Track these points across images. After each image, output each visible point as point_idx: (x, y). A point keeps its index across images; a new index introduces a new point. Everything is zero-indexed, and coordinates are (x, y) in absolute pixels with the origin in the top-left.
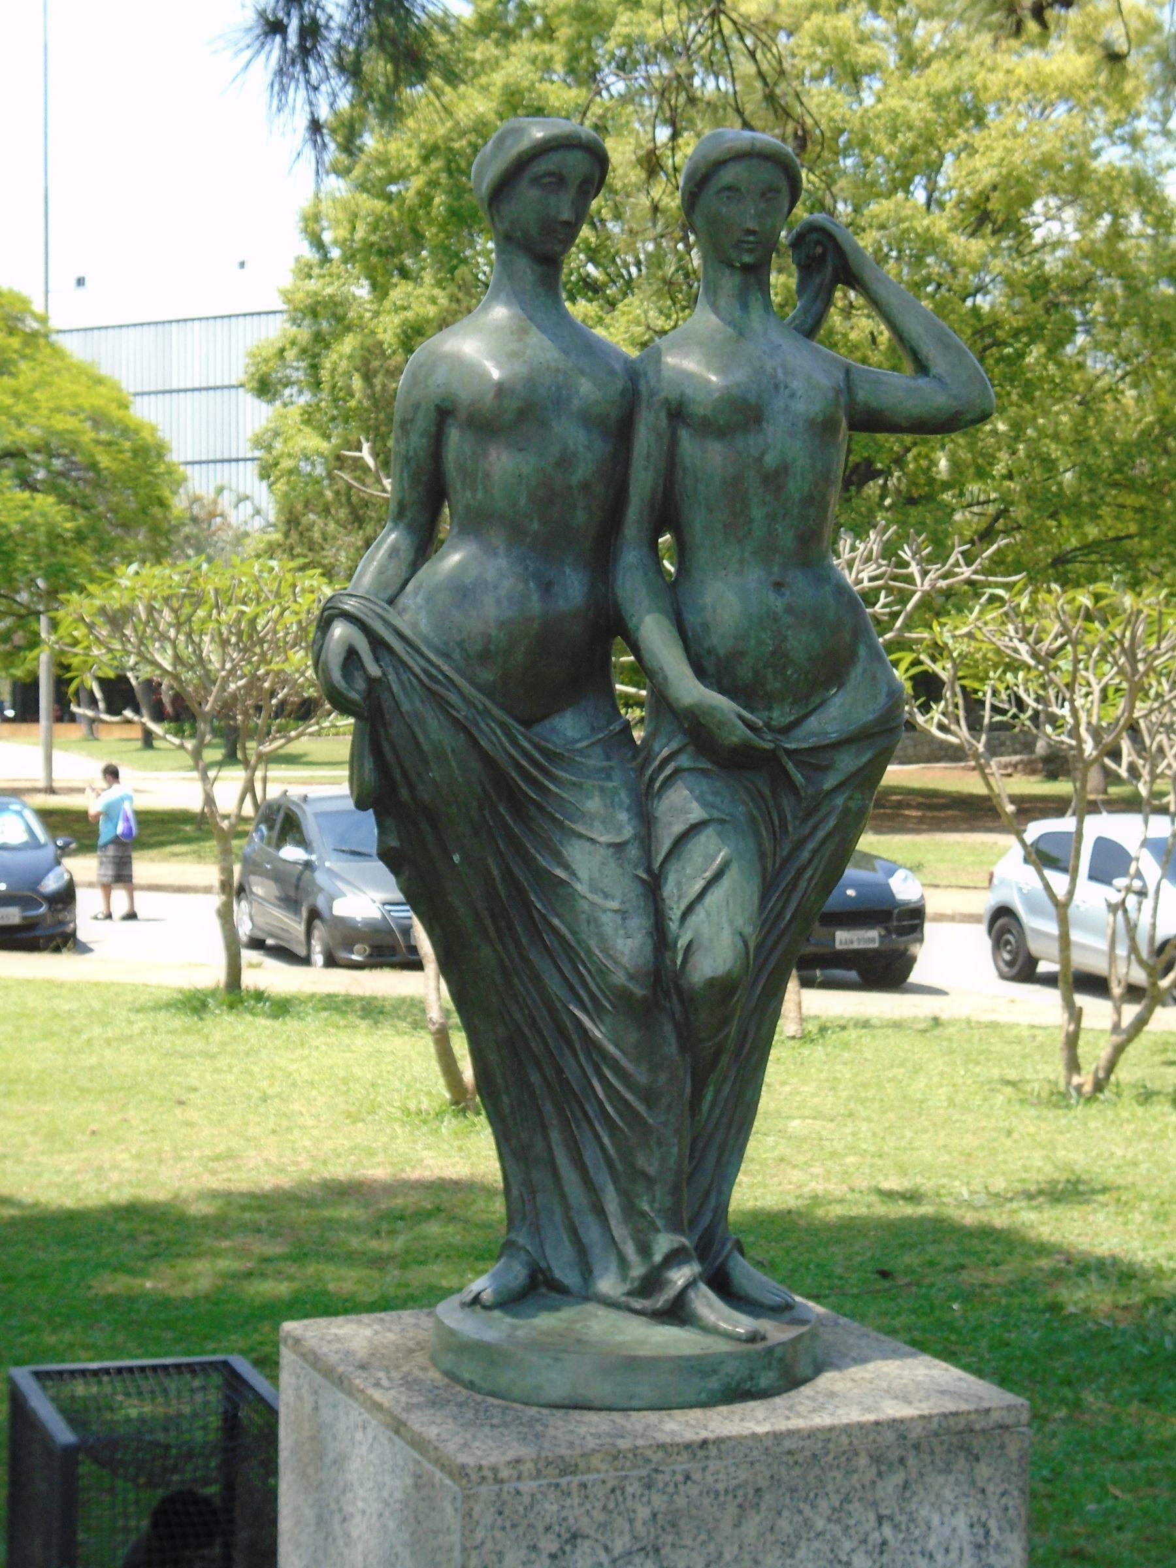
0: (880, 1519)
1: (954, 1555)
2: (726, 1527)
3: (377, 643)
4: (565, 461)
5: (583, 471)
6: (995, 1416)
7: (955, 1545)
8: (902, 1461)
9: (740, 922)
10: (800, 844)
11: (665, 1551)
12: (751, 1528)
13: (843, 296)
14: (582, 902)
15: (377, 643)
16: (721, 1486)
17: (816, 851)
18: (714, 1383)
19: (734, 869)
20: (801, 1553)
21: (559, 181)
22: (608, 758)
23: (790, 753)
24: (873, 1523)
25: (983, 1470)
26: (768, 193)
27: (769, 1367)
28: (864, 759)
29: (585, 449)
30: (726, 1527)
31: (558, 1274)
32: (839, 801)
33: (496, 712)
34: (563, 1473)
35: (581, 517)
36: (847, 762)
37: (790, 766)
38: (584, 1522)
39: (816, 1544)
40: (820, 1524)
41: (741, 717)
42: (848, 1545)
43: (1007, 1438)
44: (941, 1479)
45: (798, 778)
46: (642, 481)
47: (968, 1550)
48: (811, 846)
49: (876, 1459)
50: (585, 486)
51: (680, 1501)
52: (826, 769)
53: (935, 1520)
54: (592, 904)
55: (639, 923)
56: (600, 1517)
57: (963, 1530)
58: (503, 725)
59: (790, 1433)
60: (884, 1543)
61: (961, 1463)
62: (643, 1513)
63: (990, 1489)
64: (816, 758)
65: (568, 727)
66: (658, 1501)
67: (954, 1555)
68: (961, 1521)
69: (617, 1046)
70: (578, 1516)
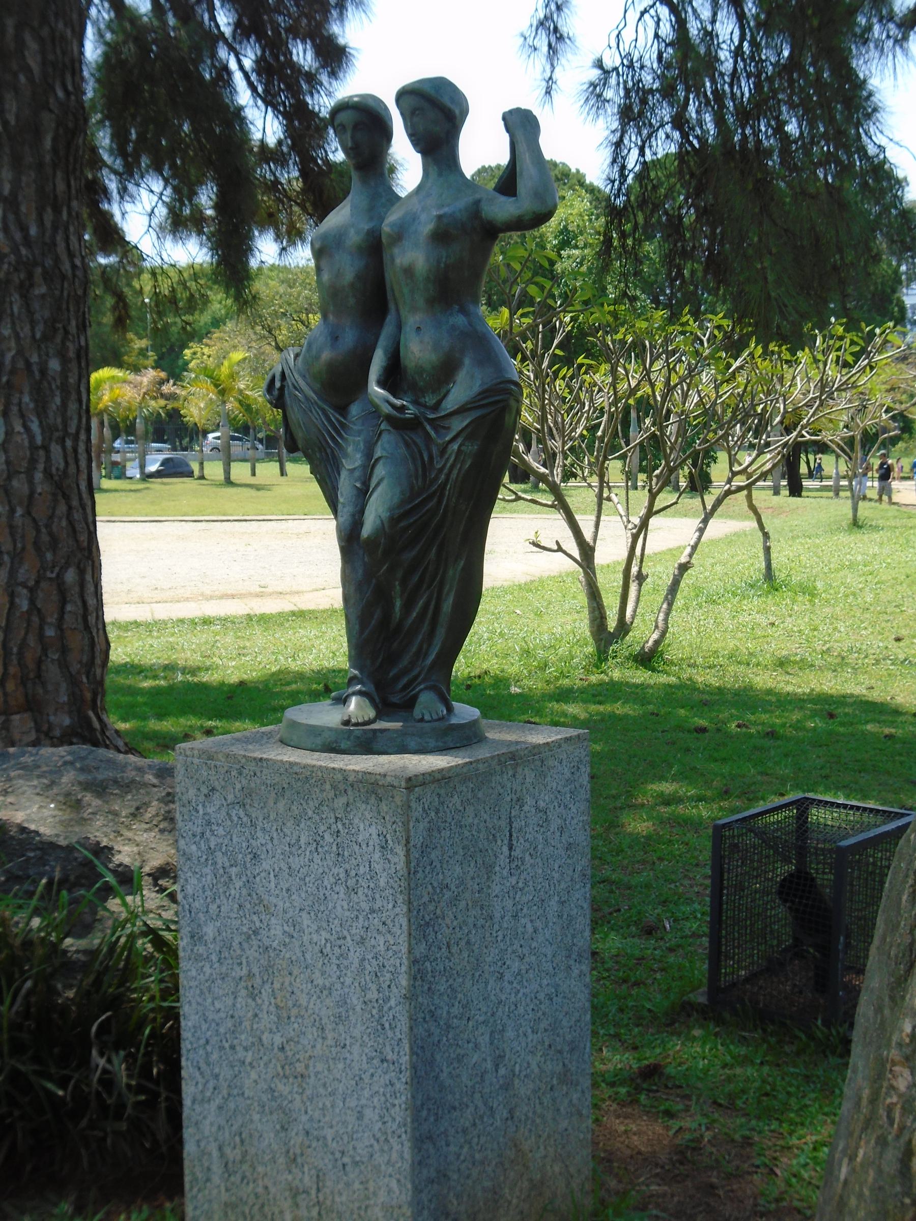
0: (337, 818)
1: (371, 848)
2: (271, 802)
6: (389, 779)
7: (371, 843)
8: (345, 791)
9: (380, 510)
10: (441, 470)
11: (247, 807)
12: (281, 805)
16: (269, 782)
17: (448, 475)
18: (319, 741)
19: (385, 482)
20: (302, 825)
22: (363, 424)
23: (428, 420)
24: (333, 820)
25: (384, 807)
27: (348, 739)
28: (465, 424)
30: (271, 802)
32: (455, 446)
33: (319, 403)
34: (209, 759)
35: (352, 301)
37: (428, 428)
38: (216, 783)
39: (308, 823)
40: (310, 813)
41: (388, 402)
42: (323, 828)
43: (395, 792)
44: (364, 806)
45: (432, 433)
47: (377, 847)
48: (446, 471)
49: (334, 787)
50: (352, 285)
51: (253, 785)
52: (448, 429)
53: (362, 828)
56: (223, 783)
57: (375, 836)
58: (323, 410)
59: (296, 764)
60: (338, 832)
61: (373, 800)
62: (238, 786)
63: (387, 818)
66: (244, 782)
67: (371, 848)
68: (373, 830)
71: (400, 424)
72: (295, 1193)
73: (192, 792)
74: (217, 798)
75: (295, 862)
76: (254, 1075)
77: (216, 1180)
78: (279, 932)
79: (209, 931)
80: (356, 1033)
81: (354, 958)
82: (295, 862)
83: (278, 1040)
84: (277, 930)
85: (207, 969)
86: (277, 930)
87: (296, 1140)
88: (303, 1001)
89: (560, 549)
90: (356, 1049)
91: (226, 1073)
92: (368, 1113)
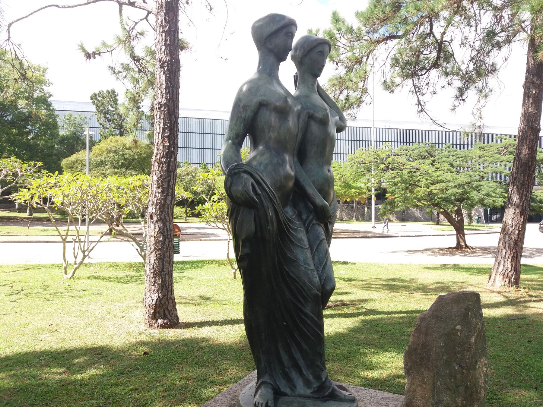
14: (302, 267)
31: (282, 390)
54: (305, 268)
69: (312, 313)
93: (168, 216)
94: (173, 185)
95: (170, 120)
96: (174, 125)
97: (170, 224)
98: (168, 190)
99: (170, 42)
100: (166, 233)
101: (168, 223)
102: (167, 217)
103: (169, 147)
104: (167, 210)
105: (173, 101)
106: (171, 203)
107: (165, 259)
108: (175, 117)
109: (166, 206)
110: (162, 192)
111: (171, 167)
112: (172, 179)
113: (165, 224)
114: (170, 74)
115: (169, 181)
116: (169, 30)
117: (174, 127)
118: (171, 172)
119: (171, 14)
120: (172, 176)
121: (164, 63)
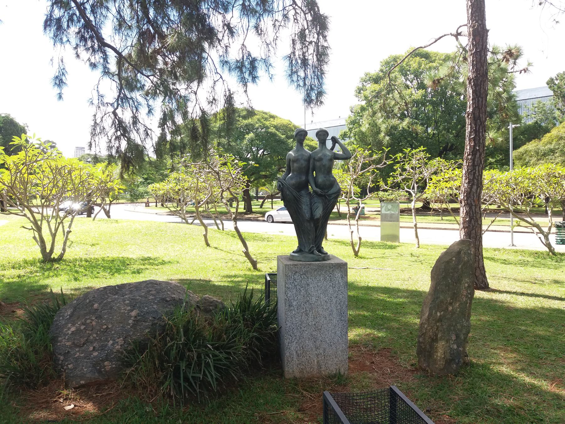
3: (282, 184)
4: (302, 164)
5: (304, 165)
12: (315, 273)
13: (337, 144)
15: (282, 184)
21: (301, 135)
26: (324, 135)
29: (304, 163)
36: (333, 196)
46: (311, 166)
55: (309, 213)
64: (330, 196)
65: (303, 192)
70: (297, 270)
71: (319, 196)
72: (317, 355)
73: (290, 274)
74: (297, 274)
75: (319, 284)
76: (307, 332)
77: (295, 359)
78: (314, 300)
79: (294, 303)
80: (335, 316)
81: (334, 301)
82: (319, 284)
83: (313, 323)
84: (314, 299)
85: (294, 312)
86: (314, 299)
87: (318, 343)
88: (321, 313)
89: (32, 229)
90: (334, 320)
91: (298, 334)
92: (337, 332)
93: (474, 201)
94: (478, 176)
95: (476, 125)
96: (479, 127)
97: (476, 208)
98: (474, 181)
99: (476, 61)
100: (472, 215)
101: (474, 208)
102: (472, 202)
103: (474, 146)
104: (472, 197)
105: (479, 108)
106: (477, 191)
107: (472, 236)
108: (480, 121)
109: (472, 193)
110: (469, 183)
111: (476, 162)
112: (477, 172)
113: (470, 208)
114: (475, 88)
115: (475, 173)
116: (476, 52)
117: (479, 129)
118: (476, 166)
119: (477, 38)
120: (477, 169)
121: (471, 80)
